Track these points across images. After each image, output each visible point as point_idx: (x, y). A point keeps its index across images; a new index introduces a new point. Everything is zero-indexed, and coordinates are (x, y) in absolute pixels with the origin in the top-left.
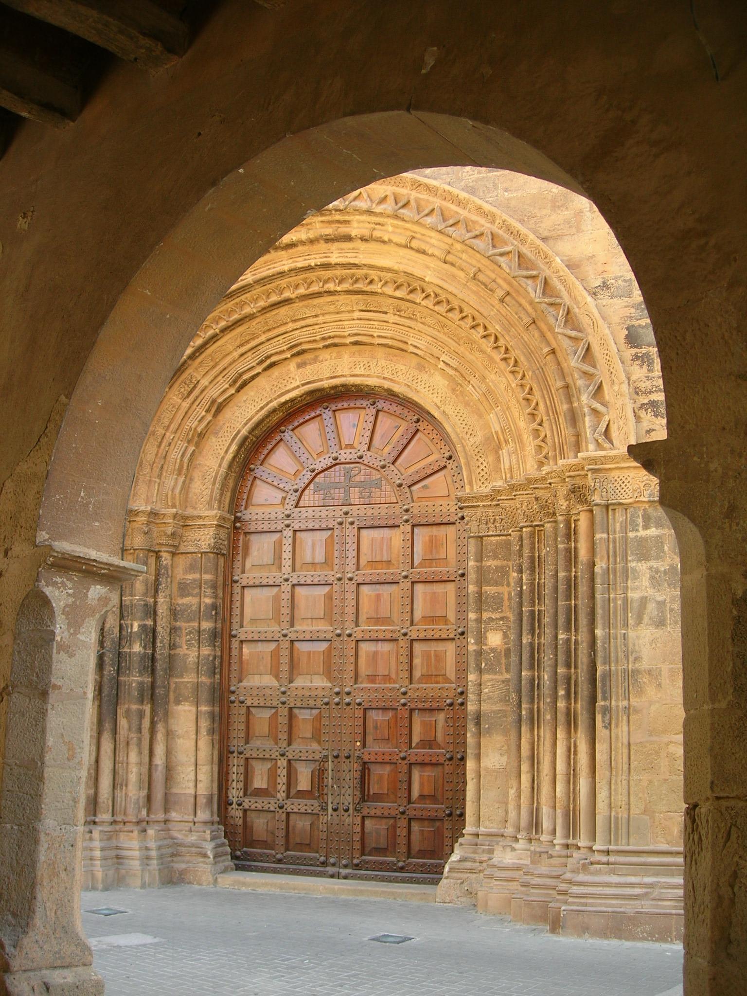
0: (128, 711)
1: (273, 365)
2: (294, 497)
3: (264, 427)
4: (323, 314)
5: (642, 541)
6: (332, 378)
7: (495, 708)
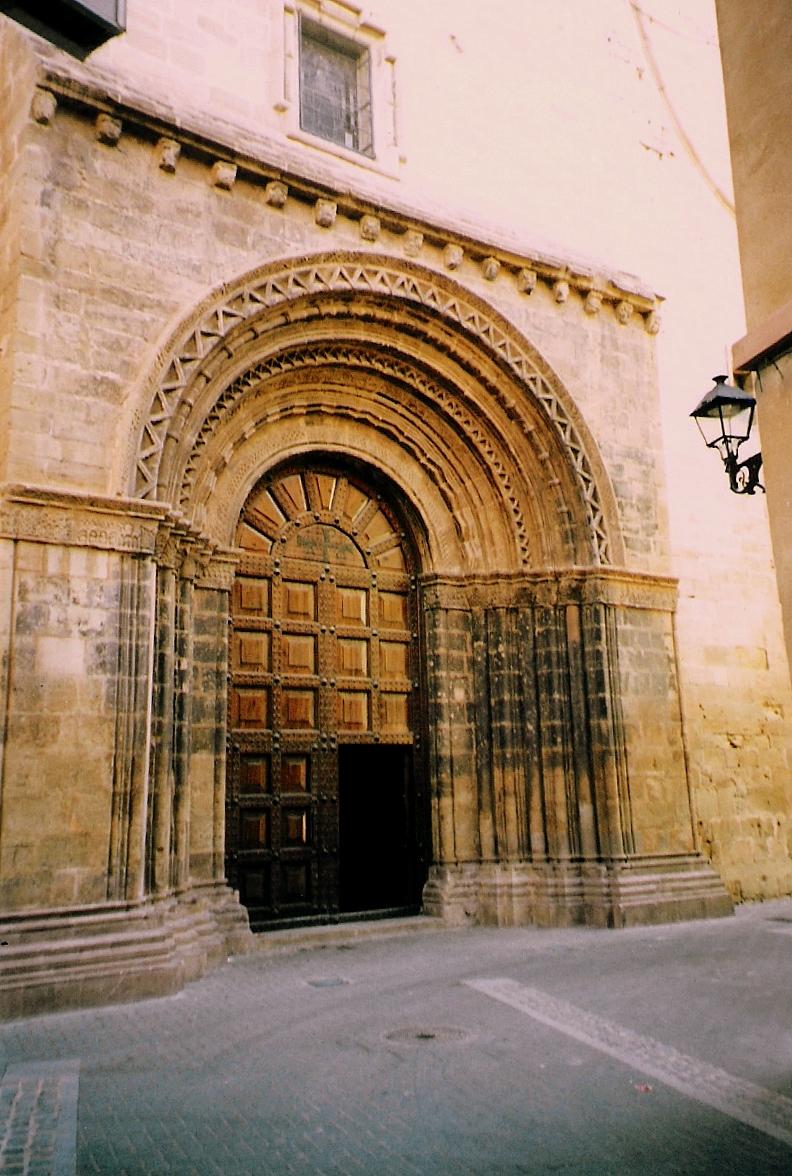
1: (290, 416)
5: (624, 632)
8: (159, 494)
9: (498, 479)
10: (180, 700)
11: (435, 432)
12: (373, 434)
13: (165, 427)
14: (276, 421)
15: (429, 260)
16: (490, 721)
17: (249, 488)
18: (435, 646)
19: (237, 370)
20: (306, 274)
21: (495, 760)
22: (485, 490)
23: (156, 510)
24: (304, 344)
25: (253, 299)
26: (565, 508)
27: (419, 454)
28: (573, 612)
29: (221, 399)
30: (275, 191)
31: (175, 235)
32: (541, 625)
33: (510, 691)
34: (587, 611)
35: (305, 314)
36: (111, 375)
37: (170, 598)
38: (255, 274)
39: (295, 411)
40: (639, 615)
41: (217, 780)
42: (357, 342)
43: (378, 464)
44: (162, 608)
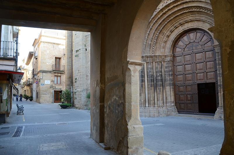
0: (159, 88)
1: (177, 27)
2: (183, 50)
3: (177, 38)
4: (184, 17)
12: (196, 22)
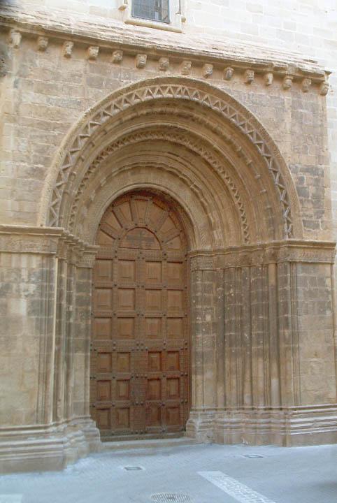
6: (146, 183)
7: (209, 349)
8: (60, 222)
9: (232, 193)
10: (69, 326)
11: (198, 170)
12: (166, 175)
13: (62, 190)
14: (116, 176)
15: (193, 76)
16: (224, 332)
17: (102, 212)
18: (196, 292)
19: (97, 153)
20: (131, 95)
21: (226, 354)
22: (224, 201)
23: (58, 232)
24: (129, 133)
25: (105, 114)
26: (269, 207)
27: (189, 183)
28: (272, 268)
29: (90, 168)
30: (116, 56)
31: (71, 88)
32: (255, 276)
33: (235, 315)
34: (280, 267)
35: (130, 117)
36: (40, 166)
37: (64, 275)
38: (106, 101)
39: (126, 168)
40: (311, 267)
41: (86, 367)
42: (157, 126)
43: (168, 191)
44: (60, 280)
